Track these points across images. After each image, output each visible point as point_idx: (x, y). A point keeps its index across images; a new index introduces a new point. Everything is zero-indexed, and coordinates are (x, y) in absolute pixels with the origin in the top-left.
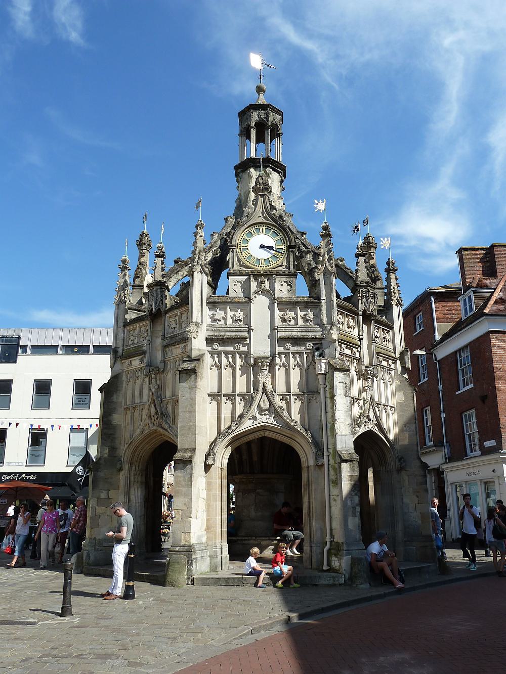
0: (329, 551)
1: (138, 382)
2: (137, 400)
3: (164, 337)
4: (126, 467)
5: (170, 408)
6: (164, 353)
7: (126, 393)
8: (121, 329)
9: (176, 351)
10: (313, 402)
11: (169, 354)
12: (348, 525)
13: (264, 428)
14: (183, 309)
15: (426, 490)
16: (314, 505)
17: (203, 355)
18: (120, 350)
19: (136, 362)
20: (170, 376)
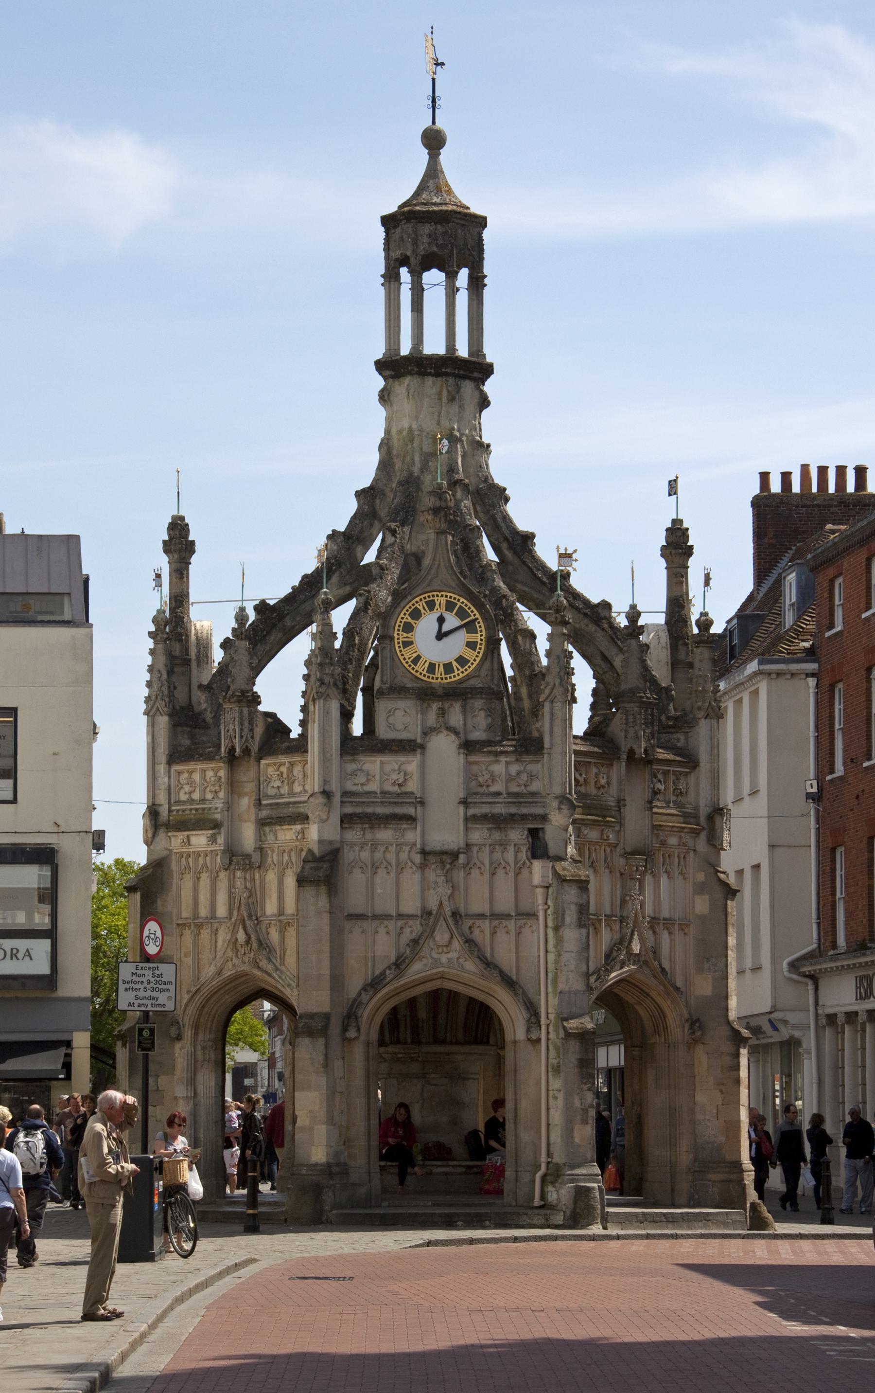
0: (544, 1178)
1: (204, 876)
2: (203, 912)
3: (258, 803)
4: (188, 1034)
5: (274, 936)
6: (260, 836)
7: (179, 896)
8: (161, 768)
9: (287, 834)
10: (526, 931)
11: (270, 837)
12: (572, 1137)
13: (442, 977)
14: (296, 758)
15: (737, 1081)
16: (524, 1104)
17: (337, 851)
18: (164, 811)
19: (200, 840)
20: (271, 877)
